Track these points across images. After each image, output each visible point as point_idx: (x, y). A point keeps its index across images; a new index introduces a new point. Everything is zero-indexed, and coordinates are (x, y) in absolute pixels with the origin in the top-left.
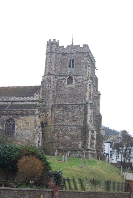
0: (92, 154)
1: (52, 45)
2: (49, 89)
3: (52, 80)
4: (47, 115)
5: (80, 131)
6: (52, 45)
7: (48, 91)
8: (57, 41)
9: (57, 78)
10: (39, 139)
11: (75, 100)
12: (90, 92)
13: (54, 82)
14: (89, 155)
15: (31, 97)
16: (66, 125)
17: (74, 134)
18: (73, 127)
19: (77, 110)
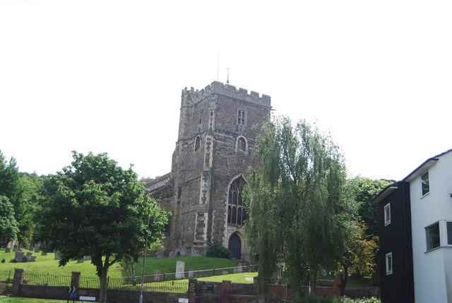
0: (198, 249)
1: (188, 95)
6: (188, 95)
8: (189, 89)
9: (187, 144)
12: (208, 154)
13: (182, 150)
14: (193, 249)
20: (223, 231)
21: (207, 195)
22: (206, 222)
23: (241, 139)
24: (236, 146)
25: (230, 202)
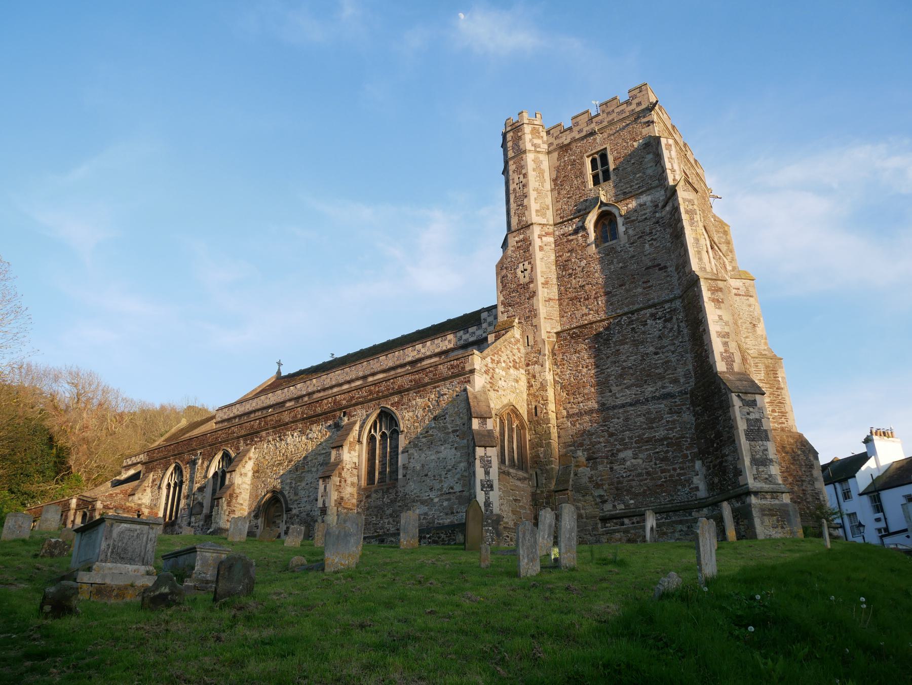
2: (527, 280)
4: (534, 377)
5: (688, 417)
7: (526, 286)
10: (487, 473)
11: (640, 290)
15: (471, 330)
16: (619, 402)
17: (661, 433)
18: (652, 407)
19: (654, 327)
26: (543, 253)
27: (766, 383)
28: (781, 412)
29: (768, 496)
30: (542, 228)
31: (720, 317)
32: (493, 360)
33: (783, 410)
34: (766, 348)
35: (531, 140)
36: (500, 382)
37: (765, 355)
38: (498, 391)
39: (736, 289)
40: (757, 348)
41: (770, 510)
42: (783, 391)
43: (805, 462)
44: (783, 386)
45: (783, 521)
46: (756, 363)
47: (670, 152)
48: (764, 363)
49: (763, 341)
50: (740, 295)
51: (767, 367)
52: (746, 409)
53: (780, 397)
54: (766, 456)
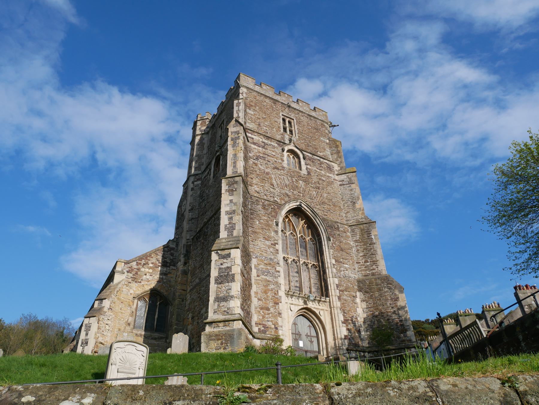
0: (217, 337)
3: (191, 185)
10: (87, 334)
13: (192, 189)
20: (277, 303)
21: (238, 219)
22: (237, 270)
23: (291, 151)
24: (285, 158)
25: (285, 250)
26: (193, 191)
27: (360, 242)
28: (373, 262)
29: (221, 324)
30: (195, 177)
31: (231, 201)
32: (138, 264)
33: (374, 259)
34: (363, 216)
35: (200, 129)
36: (145, 276)
37: (362, 222)
38: (140, 282)
39: (341, 181)
40: (355, 218)
41: (216, 335)
42: (375, 245)
43: (391, 297)
44: (375, 242)
45: (227, 344)
46: (353, 229)
47: (239, 107)
48: (360, 228)
49: (360, 212)
50: (344, 185)
51: (362, 230)
52: (222, 261)
53: (372, 250)
54: (229, 293)
